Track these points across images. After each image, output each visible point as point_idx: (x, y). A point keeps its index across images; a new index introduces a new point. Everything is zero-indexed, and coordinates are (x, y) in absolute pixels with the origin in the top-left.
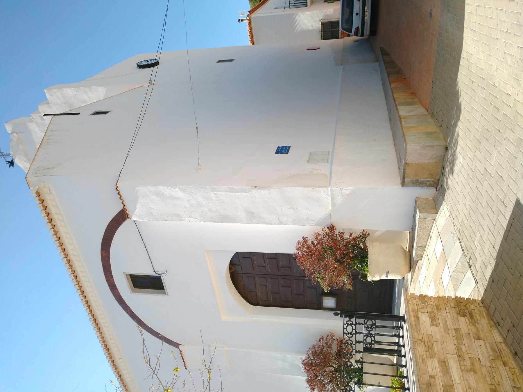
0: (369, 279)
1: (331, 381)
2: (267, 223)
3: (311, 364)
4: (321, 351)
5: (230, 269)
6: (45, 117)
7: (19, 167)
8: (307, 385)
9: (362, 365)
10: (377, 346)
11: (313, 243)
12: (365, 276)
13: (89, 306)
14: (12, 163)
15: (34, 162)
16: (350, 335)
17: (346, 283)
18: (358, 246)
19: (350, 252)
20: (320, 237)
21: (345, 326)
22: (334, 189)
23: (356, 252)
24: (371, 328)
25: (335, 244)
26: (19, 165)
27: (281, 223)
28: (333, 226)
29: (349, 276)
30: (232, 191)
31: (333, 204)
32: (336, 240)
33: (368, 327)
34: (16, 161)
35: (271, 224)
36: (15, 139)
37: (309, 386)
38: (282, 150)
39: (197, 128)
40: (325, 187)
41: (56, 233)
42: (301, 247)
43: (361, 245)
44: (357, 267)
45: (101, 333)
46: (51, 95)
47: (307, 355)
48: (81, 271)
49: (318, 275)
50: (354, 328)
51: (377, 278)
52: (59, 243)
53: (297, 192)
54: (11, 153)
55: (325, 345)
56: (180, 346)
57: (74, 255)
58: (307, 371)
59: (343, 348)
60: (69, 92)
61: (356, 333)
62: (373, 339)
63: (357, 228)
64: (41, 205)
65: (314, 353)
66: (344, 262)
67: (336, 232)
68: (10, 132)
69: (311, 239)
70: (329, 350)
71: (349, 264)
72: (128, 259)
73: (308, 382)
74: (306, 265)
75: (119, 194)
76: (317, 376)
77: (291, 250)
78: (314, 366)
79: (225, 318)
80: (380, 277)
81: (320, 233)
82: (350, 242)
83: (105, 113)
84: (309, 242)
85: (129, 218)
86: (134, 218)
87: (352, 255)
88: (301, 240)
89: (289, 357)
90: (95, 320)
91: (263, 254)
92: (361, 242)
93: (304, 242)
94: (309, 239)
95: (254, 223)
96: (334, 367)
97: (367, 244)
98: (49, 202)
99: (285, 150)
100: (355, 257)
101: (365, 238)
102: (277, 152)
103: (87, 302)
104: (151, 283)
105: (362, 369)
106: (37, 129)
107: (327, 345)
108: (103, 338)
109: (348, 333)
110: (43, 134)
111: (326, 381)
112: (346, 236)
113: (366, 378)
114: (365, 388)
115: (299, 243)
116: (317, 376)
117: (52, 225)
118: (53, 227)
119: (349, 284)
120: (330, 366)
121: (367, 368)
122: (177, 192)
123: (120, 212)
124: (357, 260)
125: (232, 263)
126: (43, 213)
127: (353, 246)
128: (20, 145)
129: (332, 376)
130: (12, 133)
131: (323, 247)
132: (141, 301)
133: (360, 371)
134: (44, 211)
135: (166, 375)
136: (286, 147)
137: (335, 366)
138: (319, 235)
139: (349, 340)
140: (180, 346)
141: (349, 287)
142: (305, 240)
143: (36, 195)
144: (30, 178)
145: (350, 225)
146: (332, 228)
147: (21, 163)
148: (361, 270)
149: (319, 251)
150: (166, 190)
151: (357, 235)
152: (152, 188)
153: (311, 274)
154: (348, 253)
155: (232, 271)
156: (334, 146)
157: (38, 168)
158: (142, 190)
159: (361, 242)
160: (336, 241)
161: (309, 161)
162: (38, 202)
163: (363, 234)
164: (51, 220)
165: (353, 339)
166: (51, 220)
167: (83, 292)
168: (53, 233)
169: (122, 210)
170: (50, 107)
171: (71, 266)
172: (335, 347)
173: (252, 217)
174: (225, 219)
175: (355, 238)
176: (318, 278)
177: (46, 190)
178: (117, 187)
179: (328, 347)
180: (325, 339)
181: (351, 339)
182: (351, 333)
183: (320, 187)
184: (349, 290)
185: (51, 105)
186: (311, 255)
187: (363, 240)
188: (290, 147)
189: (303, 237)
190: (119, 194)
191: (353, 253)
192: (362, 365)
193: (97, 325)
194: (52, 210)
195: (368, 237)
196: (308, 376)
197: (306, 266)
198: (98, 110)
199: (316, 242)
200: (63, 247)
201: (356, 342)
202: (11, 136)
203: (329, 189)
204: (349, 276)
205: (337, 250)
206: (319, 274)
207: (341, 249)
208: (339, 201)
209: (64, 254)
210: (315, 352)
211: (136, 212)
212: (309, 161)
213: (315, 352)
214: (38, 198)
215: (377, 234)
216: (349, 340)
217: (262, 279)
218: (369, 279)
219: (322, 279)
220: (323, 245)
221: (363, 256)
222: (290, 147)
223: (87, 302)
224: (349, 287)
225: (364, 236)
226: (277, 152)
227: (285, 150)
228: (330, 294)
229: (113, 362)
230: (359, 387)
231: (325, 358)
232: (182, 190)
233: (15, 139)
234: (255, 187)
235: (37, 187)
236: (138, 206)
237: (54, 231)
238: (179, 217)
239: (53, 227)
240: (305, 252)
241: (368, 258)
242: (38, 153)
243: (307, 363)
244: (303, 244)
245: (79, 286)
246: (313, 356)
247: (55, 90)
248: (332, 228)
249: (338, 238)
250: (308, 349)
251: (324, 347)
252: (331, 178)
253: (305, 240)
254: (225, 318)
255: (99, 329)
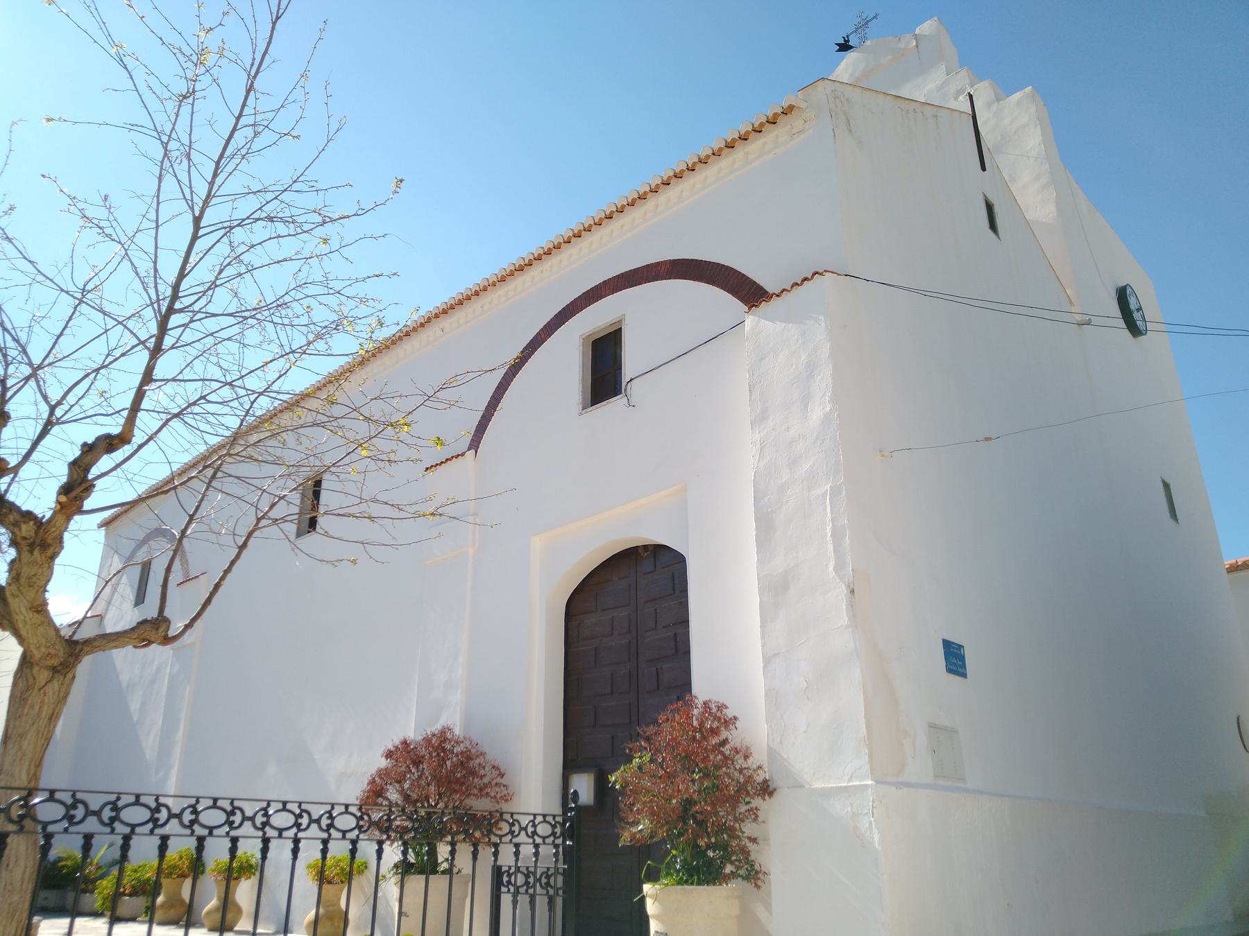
0: (647, 888)
1: (407, 798)
2: (763, 626)
3: (444, 750)
4: (472, 773)
5: (646, 547)
6: (963, 99)
7: (839, 64)
8: (397, 742)
9: (443, 872)
10: (506, 900)
11: (724, 742)
12: (653, 877)
13: (548, 253)
14: (845, 47)
15: (858, 91)
16: (530, 829)
17: (634, 830)
18: (726, 858)
19: (709, 839)
20: (740, 762)
21: (549, 819)
22: (870, 795)
23: (710, 854)
24: (548, 884)
25: (727, 800)
26: (843, 63)
27: (767, 661)
28: (771, 794)
29: (652, 837)
30: (837, 535)
31: (826, 793)
32: (738, 801)
33: (548, 877)
34: (851, 56)
35: (763, 637)
36: (902, 45)
37: (397, 747)
38: (954, 658)
39: (988, 439)
40: (872, 769)
41: (703, 161)
42: (710, 714)
43: (729, 869)
44: (675, 857)
45: (494, 284)
46: (1019, 102)
47: (461, 738)
48: (706, 178)
49: (647, 758)
50: (547, 841)
51: (651, 907)
52: (747, 133)
53: (850, 695)
54: (868, 43)
55: (486, 780)
56: (473, 451)
57: (657, 206)
58: (427, 740)
59: (480, 827)
60: (1034, 140)
61: (537, 846)
62: (522, 890)
63: (770, 857)
64: (764, 120)
65: (467, 756)
66: (685, 823)
67: (757, 802)
68: (917, 31)
69: (736, 737)
70: (476, 791)
71: (680, 834)
72: (649, 319)
73: (405, 743)
74: (668, 729)
75: (806, 279)
76: (417, 762)
77: (704, 685)
78: (438, 755)
79: (537, 542)
80: (656, 917)
81: (750, 761)
82: (733, 836)
83: (993, 226)
84: (724, 734)
85: (750, 309)
86: (750, 320)
87: (702, 843)
88: (729, 713)
89: (457, 697)
90: (521, 269)
91: (685, 622)
92: (738, 868)
93: (726, 721)
94: (734, 732)
95: (760, 595)
96: (437, 804)
97: (733, 884)
98: (770, 136)
99: (955, 665)
100: (699, 853)
101: (746, 878)
102: (947, 644)
103: (558, 247)
104: (605, 373)
105: (435, 872)
106: (931, 85)
107: (486, 786)
108: (485, 289)
109: (534, 826)
110: (923, 100)
111: (406, 786)
112: (749, 829)
113: (416, 882)
114: (393, 880)
115: (721, 707)
116: (417, 762)
117: (720, 150)
118: (717, 154)
119: (633, 836)
120: (440, 795)
121: (439, 883)
122: (820, 408)
123: (761, 288)
124: (693, 858)
125: (659, 550)
126: (744, 128)
127: (724, 847)
128: (889, 57)
129: (417, 801)
130: (916, 36)
131: (718, 767)
132: (566, 357)
133: (428, 867)
134: (750, 129)
135: (428, 423)
136: (964, 666)
137: (441, 805)
138: (746, 757)
139: (521, 829)
140: (473, 451)
141: (625, 839)
142: (729, 723)
143: (785, 106)
144: (822, 90)
145: (778, 835)
146: (766, 790)
147: (847, 67)
148: (668, 866)
149: (705, 759)
150: (823, 382)
151: (752, 857)
152: (825, 351)
153: (648, 739)
154: (708, 834)
155: (640, 551)
156: (983, 793)
157: (848, 100)
158: (819, 330)
159: (738, 868)
160: (734, 801)
161: (932, 726)
162: (770, 114)
163: (757, 872)
164: (730, 146)
165: (522, 838)
166: (730, 146)
167: (539, 258)
168: (703, 155)
169: (766, 292)
170: (989, 105)
171: (632, 204)
172: (480, 805)
173: (776, 589)
174: (765, 524)
175: (746, 853)
176: (641, 758)
177: (798, 124)
178: (821, 274)
179: (481, 790)
180: (499, 780)
181: (523, 833)
182: (534, 833)
183: (871, 756)
184: (618, 837)
185: (995, 106)
186: (694, 738)
187: (741, 872)
188: (964, 675)
189: (735, 718)
190: (806, 279)
191: (708, 847)
192: (443, 872)
193: (512, 274)
194: (755, 145)
195: (749, 886)
196: (416, 743)
197: (666, 727)
198: (997, 209)
199: (726, 750)
200: (673, 181)
201: (517, 846)
202: (908, 36)
203: (870, 782)
204: (652, 837)
205: (713, 805)
206: (651, 761)
207: (716, 814)
208: (840, 808)
209: (657, 186)
210: (470, 758)
211: (767, 325)
212: (932, 726)
213: (470, 758)
214: (779, 111)
215: (761, 911)
216: (521, 829)
217: (627, 625)
218: (647, 888)
219: (640, 768)
220: (720, 767)
221: (703, 871)
222: (964, 675)
223: (558, 247)
224: (625, 839)
225: (753, 875)
226: (947, 644)
227: (955, 665)
228: (601, 787)
229: (437, 316)
230: (396, 866)
231: (457, 781)
232: (827, 418)
233: (902, 45)
234: (852, 592)
235: (803, 105)
236: (779, 326)
237: (708, 157)
238: (760, 419)
239: (717, 154)
240: (702, 724)
241: (698, 884)
242: (882, 96)
243: (445, 740)
244: (719, 719)
245: (590, 226)
246: (462, 752)
247: (1033, 109)
248: (766, 790)
249: (743, 808)
250: (475, 740)
251: (482, 777)
252: (899, 785)
253: (729, 723)
254: (537, 542)
255: (503, 279)
